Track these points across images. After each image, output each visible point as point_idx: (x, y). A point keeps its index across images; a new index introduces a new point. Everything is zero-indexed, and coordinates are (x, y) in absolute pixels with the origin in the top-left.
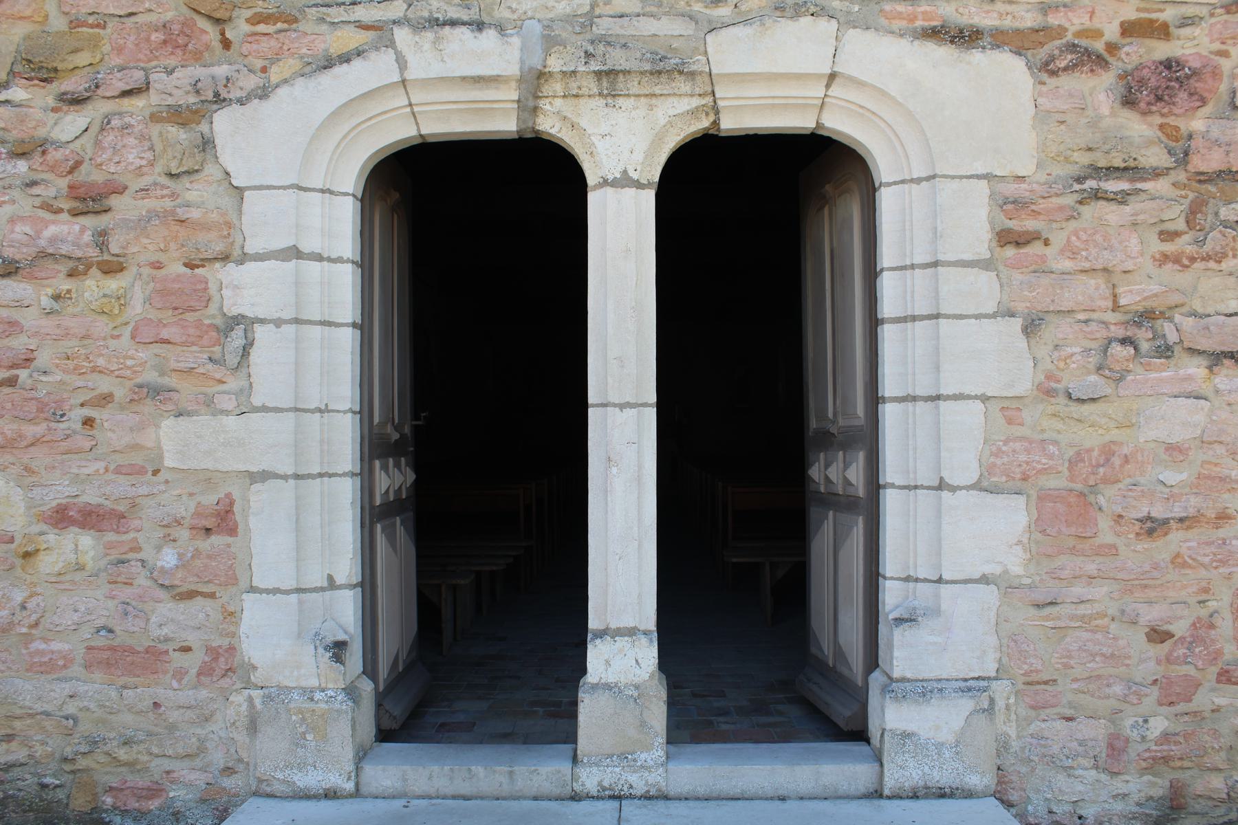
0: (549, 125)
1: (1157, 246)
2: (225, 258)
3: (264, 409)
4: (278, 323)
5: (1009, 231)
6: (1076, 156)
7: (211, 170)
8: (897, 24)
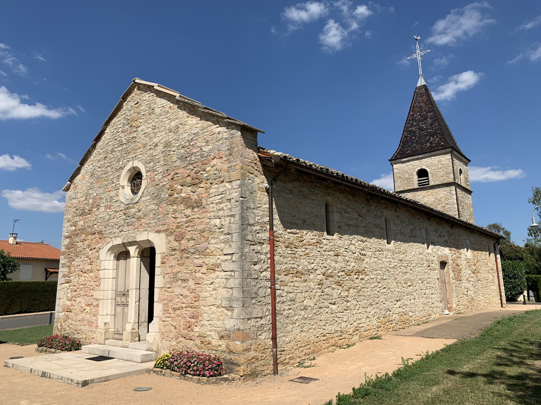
4: (103, 278)
6: (170, 248)
7: (99, 259)
8: (154, 231)
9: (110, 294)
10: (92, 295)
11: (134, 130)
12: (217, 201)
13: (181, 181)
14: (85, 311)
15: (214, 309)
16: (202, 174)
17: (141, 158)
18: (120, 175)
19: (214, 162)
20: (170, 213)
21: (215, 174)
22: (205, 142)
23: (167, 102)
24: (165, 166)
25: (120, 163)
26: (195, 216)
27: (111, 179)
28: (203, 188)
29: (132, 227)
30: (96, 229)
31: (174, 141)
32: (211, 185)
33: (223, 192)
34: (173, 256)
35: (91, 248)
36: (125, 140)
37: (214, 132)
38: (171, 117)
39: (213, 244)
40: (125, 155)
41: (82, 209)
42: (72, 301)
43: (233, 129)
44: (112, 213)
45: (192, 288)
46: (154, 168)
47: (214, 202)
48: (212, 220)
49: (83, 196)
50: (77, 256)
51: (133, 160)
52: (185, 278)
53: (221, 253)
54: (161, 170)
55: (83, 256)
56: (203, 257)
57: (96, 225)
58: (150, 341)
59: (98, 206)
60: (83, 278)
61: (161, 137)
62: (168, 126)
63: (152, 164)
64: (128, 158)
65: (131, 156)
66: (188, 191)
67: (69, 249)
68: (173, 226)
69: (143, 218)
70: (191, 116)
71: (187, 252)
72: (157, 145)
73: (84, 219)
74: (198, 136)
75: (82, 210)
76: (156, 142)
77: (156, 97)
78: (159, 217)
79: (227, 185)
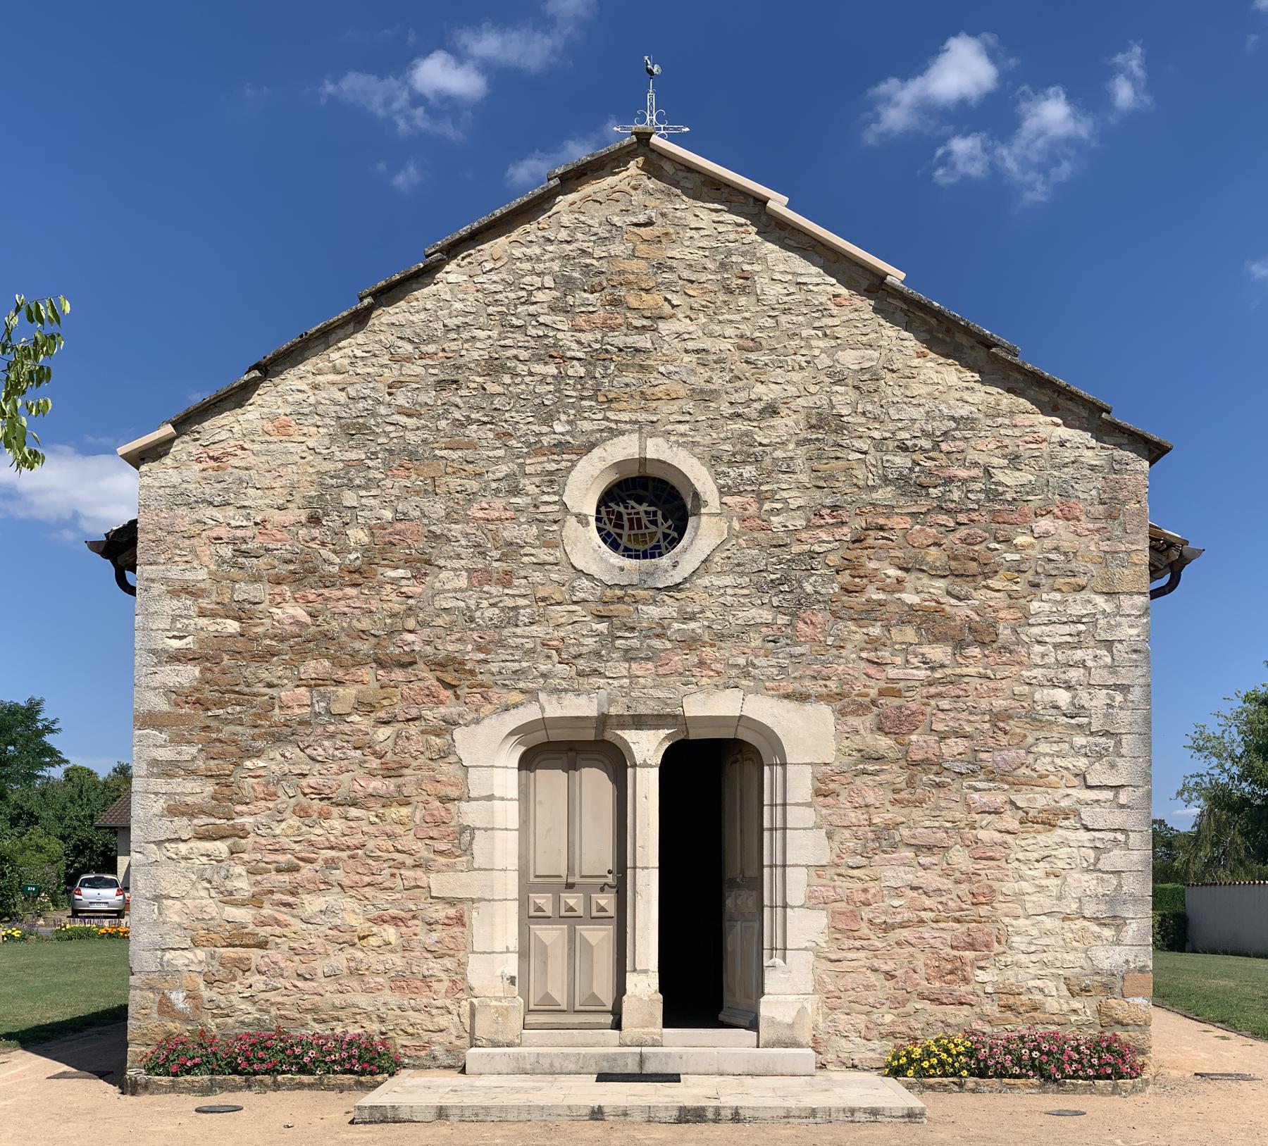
0: (608, 735)
1: (891, 796)
2: (459, 799)
3: (480, 869)
4: (486, 830)
5: (820, 789)
6: (854, 753)
7: (452, 759)
9: (510, 885)
10: (418, 887)
12: (1058, 639)
14: (373, 941)
15: (1049, 923)
16: (997, 549)
17: (683, 435)
18: (564, 473)
19: (1044, 524)
20: (849, 646)
21: (1050, 560)
22: (1004, 457)
23: (819, 275)
24: (818, 493)
25: (559, 428)
28: (998, 591)
29: (650, 665)
30: (417, 648)
31: (863, 420)
33: (1082, 617)
34: (871, 777)
35: (382, 714)
36: (575, 346)
38: (841, 332)
39: (1045, 755)
40: (586, 403)
41: (289, 556)
43: (1120, 446)
45: (964, 868)
46: (763, 488)
47: (1047, 639)
48: (1038, 688)
49: (289, 505)
50: (277, 739)
51: (641, 433)
52: (932, 842)
53: (1076, 781)
54: (801, 502)
55: (326, 743)
56: (1006, 787)
57: (410, 632)
58: (779, 1018)
59: (421, 565)
60: (337, 824)
61: (792, 390)
62: (823, 361)
63: (749, 471)
64: (606, 419)
65: (625, 416)
66: (932, 590)
68: (865, 686)
69: (711, 646)
70: (933, 355)
71: (935, 768)
72: (771, 410)
73: (311, 597)
74: (972, 429)
76: (765, 398)
77: (759, 239)
78: (798, 650)
79: (1100, 600)
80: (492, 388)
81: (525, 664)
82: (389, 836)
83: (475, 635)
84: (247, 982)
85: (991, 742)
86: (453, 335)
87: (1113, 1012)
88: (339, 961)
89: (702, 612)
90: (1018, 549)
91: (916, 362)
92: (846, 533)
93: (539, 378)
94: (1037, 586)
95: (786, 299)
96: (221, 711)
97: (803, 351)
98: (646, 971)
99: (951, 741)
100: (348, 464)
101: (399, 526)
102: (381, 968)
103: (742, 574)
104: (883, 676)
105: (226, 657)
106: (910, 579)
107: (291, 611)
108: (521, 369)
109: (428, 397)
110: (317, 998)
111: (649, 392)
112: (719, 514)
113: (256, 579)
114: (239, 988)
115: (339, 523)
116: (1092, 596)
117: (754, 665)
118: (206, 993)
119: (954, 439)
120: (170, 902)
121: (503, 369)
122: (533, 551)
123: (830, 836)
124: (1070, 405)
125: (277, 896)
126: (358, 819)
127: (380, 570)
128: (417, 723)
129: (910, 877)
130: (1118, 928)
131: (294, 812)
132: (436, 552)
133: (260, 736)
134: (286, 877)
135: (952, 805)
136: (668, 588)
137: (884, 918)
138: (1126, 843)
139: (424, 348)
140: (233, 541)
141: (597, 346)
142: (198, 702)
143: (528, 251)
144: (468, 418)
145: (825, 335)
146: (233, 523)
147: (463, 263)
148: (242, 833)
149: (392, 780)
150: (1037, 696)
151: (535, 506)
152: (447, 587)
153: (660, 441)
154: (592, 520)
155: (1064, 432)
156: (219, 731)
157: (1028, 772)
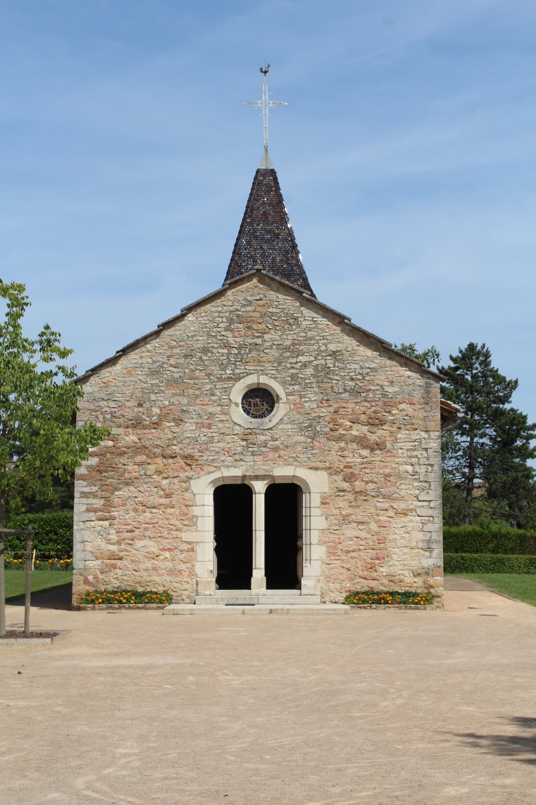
0: (246, 482)
1: (349, 504)
2: (192, 506)
4: (202, 517)
7: (190, 491)
10: (177, 538)
11: (257, 335)
13: (349, 417)
14: (161, 557)
15: (406, 550)
19: (403, 406)
20: (333, 450)
21: (405, 419)
22: (388, 382)
25: (228, 372)
26: (377, 459)
27: (207, 389)
29: (261, 457)
30: (177, 451)
31: (337, 369)
32: (399, 430)
36: (234, 343)
37: (402, 374)
38: (329, 338)
39: (403, 489)
40: (238, 363)
41: (131, 418)
42: (122, 544)
43: (429, 378)
44: (215, 434)
46: (302, 393)
50: (127, 484)
52: (363, 521)
53: (415, 499)
54: (315, 398)
55: (145, 486)
59: (179, 421)
60: (148, 515)
63: (297, 387)
64: (245, 369)
65: (252, 368)
67: (100, 471)
69: (284, 450)
71: (364, 494)
72: (305, 365)
73: (139, 433)
74: (377, 372)
75: (132, 420)
78: (314, 452)
79: (423, 434)
80: (204, 358)
81: (216, 457)
82: (167, 519)
83: (198, 447)
84: (116, 572)
85: (384, 485)
86: (190, 339)
87: (429, 583)
88: (149, 564)
89: (280, 438)
90: (393, 415)
91: (356, 348)
92: (332, 409)
93: (221, 354)
94: (400, 428)
95: (309, 326)
96: (106, 474)
97: (316, 345)
98: (260, 568)
99: (370, 484)
100: (152, 385)
101: (171, 407)
102: (164, 567)
103: (294, 424)
104: (345, 461)
105: (108, 455)
106: (355, 426)
107: (132, 438)
108: (215, 351)
109: (182, 361)
110: (140, 578)
111: (261, 359)
112: (285, 403)
113: (120, 426)
114: (112, 574)
115: (149, 406)
116: (420, 432)
117: (299, 457)
118: (100, 576)
119: (370, 375)
120: (88, 543)
121: (209, 351)
122: (219, 416)
123: (326, 519)
124: (412, 363)
125: (126, 541)
126: (156, 513)
127: (164, 423)
128: (177, 478)
129: (356, 533)
130: (431, 552)
131: (133, 510)
132: (184, 417)
133: (121, 483)
134: (129, 534)
135: (370, 507)
136: (267, 429)
137: (346, 548)
138: (433, 521)
139: (180, 343)
140: (111, 413)
141: (242, 343)
142: (98, 470)
143: (217, 309)
144: (196, 368)
145: (324, 338)
146: (111, 406)
147: (194, 313)
148: (114, 518)
149: (168, 499)
150: (401, 468)
151: (220, 400)
152: (188, 429)
153: (265, 376)
154: (240, 405)
155: (409, 373)
156: (106, 481)
157: (397, 495)
